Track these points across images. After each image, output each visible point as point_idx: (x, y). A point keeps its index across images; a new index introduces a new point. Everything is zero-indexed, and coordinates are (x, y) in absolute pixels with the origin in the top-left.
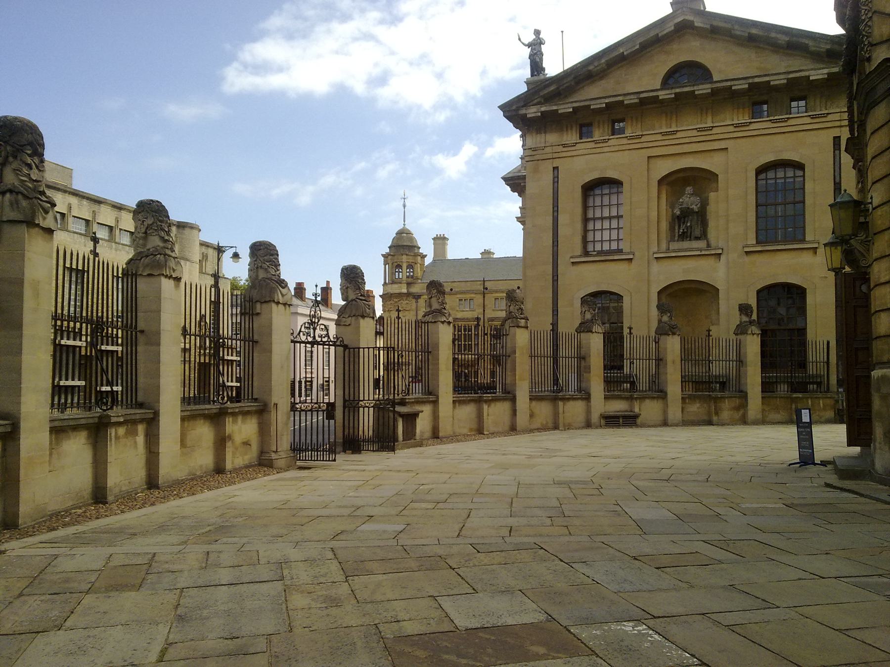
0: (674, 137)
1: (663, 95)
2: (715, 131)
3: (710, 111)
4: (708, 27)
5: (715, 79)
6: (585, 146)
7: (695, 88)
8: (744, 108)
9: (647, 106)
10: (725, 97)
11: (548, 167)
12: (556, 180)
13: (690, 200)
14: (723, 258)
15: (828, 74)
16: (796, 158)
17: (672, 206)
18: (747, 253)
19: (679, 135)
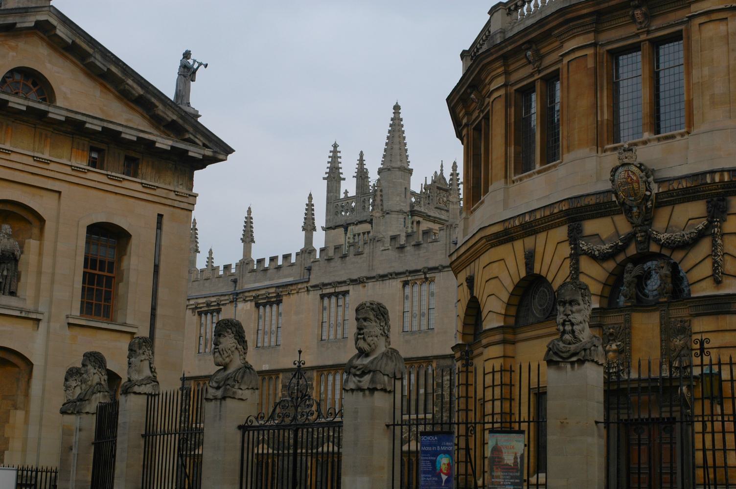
0: (7, 157)
2: (52, 166)
3: (49, 140)
4: (70, 41)
5: (58, 104)
7: (51, 109)
8: (83, 150)
10: (74, 130)
14: (42, 325)
15: (172, 147)
16: (41, 212)
18: (70, 325)
19: (13, 157)
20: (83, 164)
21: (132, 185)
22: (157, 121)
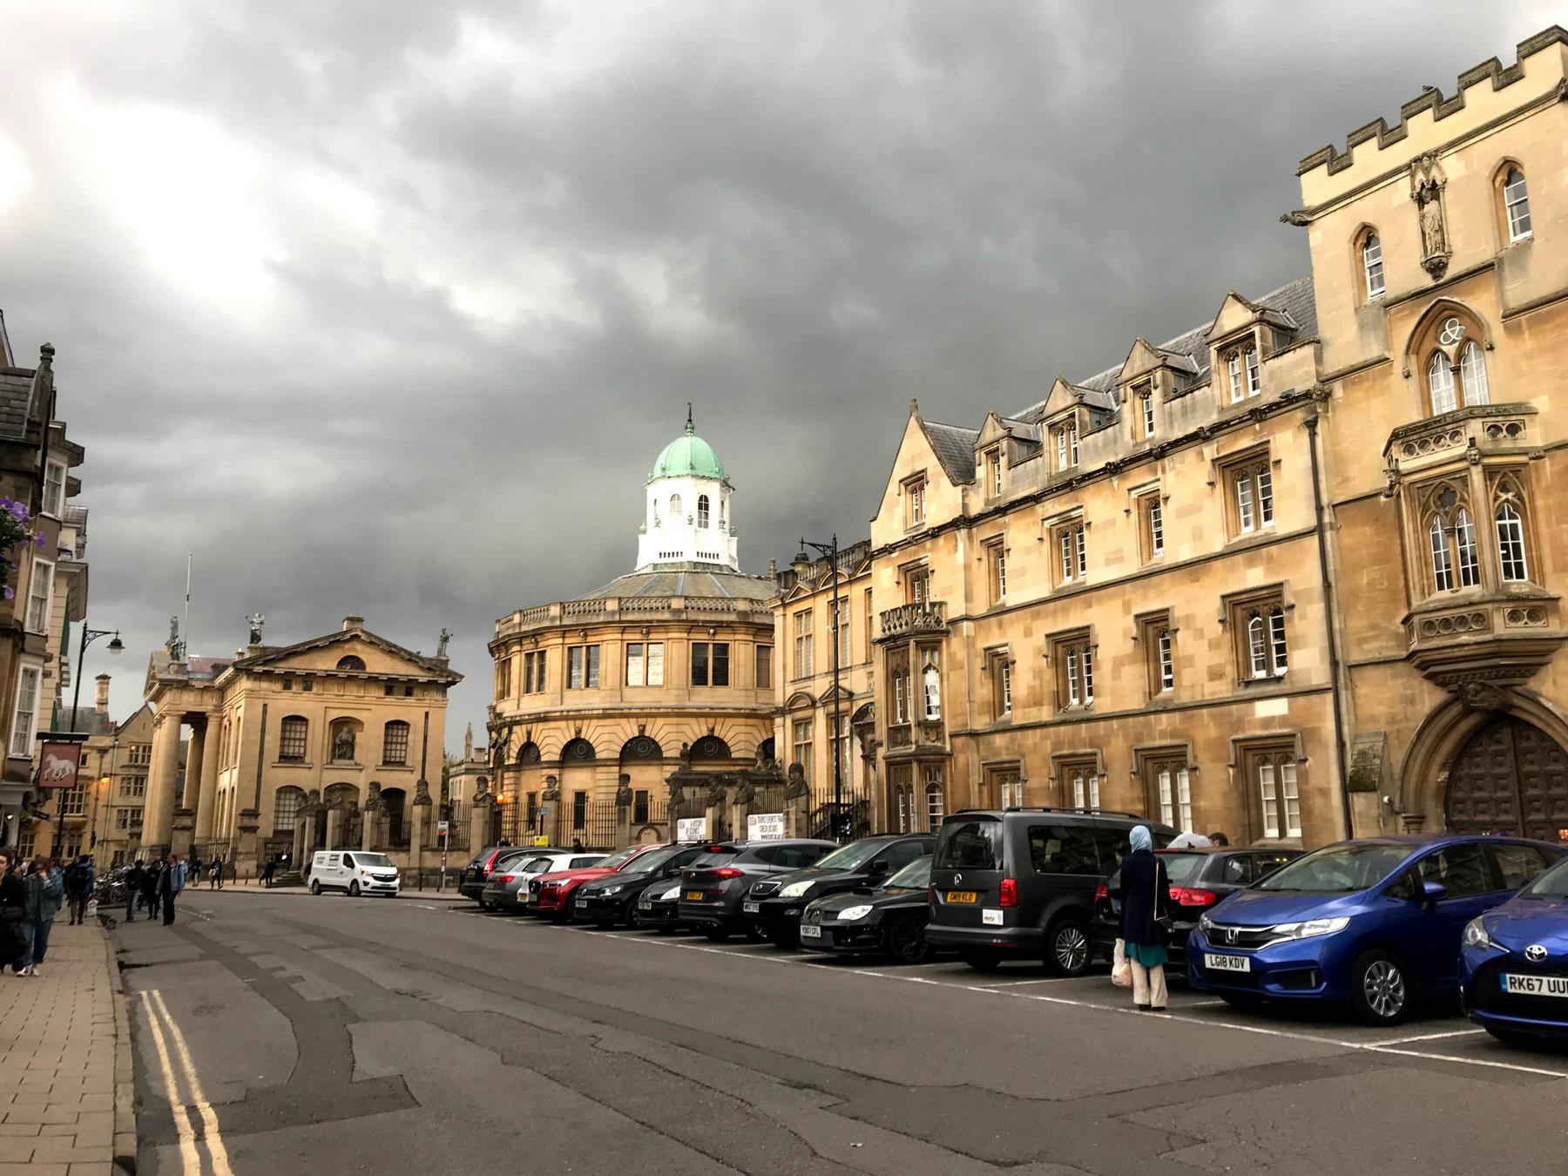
1: (341, 675)
6: (287, 694)
9: (330, 677)
10: (373, 680)
11: (261, 703)
12: (265, 712)
13: (344, 735)
17: (334, 737)
20: (382, 694)
21: (410, 700)
22: (421, 668)
